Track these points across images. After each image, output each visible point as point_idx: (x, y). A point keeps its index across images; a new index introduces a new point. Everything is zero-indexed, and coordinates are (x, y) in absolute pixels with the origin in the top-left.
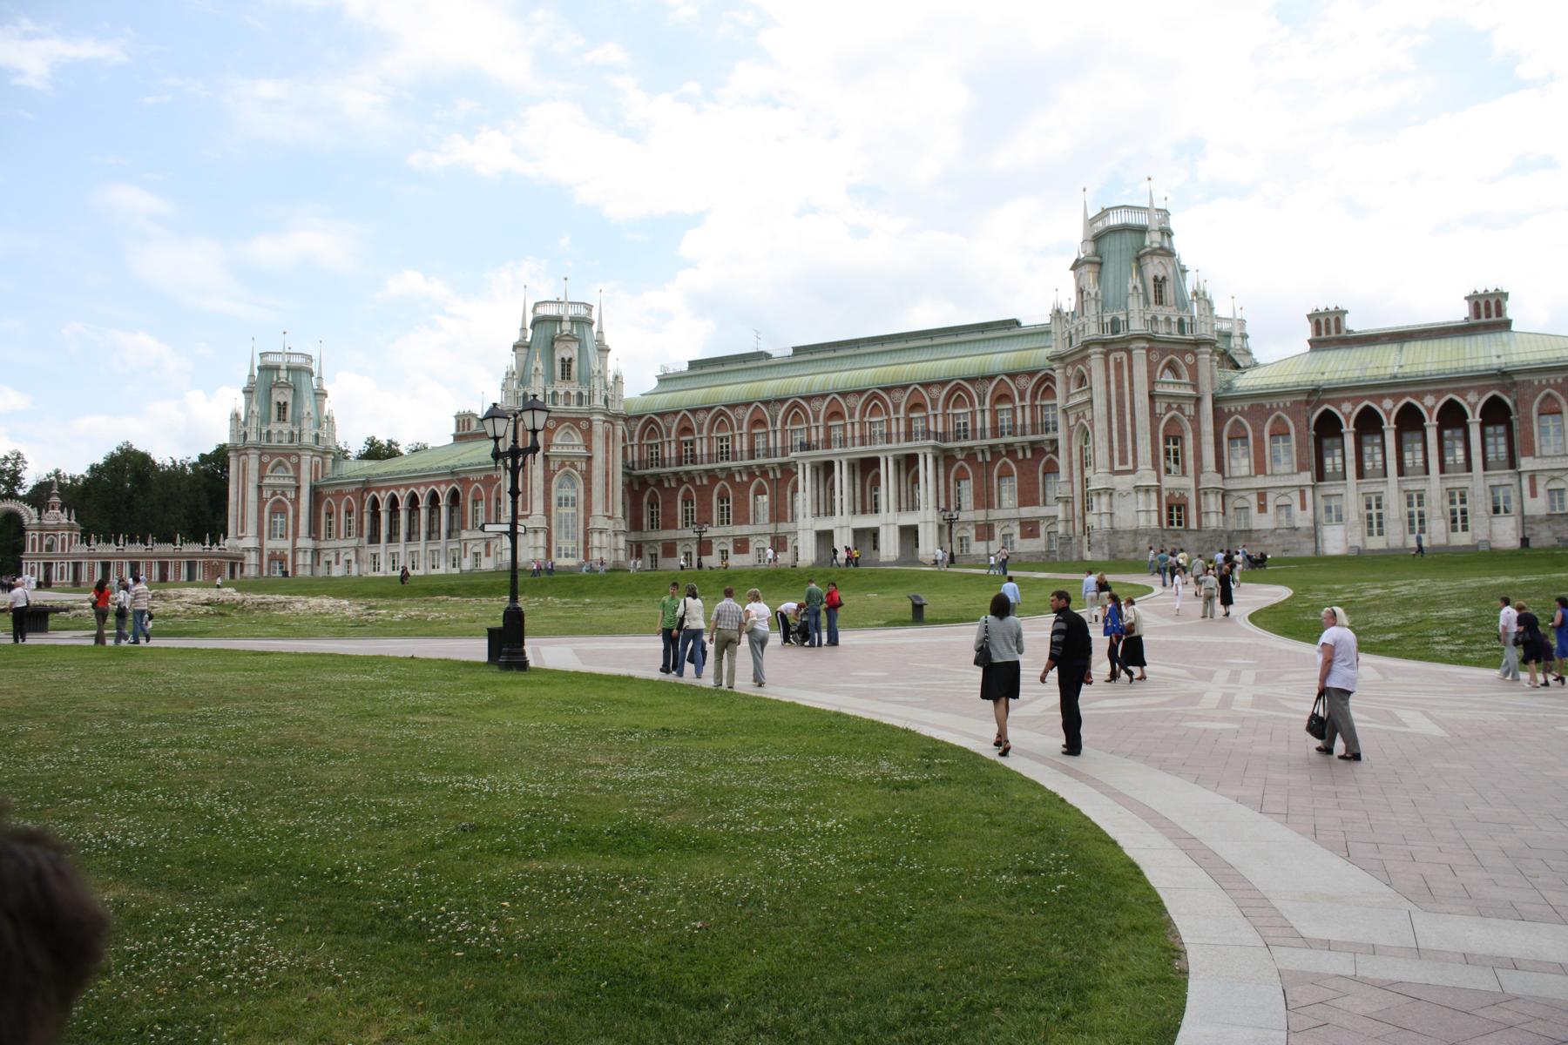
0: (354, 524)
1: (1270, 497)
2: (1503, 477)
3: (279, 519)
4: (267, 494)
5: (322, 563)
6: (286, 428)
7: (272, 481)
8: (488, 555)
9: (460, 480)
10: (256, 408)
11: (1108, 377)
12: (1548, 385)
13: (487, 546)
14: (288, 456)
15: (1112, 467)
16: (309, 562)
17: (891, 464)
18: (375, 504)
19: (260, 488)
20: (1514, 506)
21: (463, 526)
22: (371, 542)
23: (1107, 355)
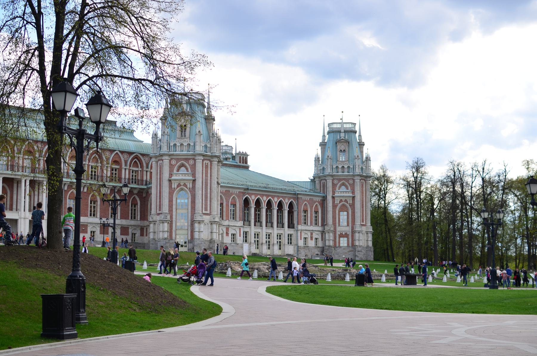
1: (230, 229)
2: (291, 231)
11: (203, 170)
12: (306, 200)
15: (202, 211)
17: (28, 183)
20: (294, 241)
23: (203, 160)
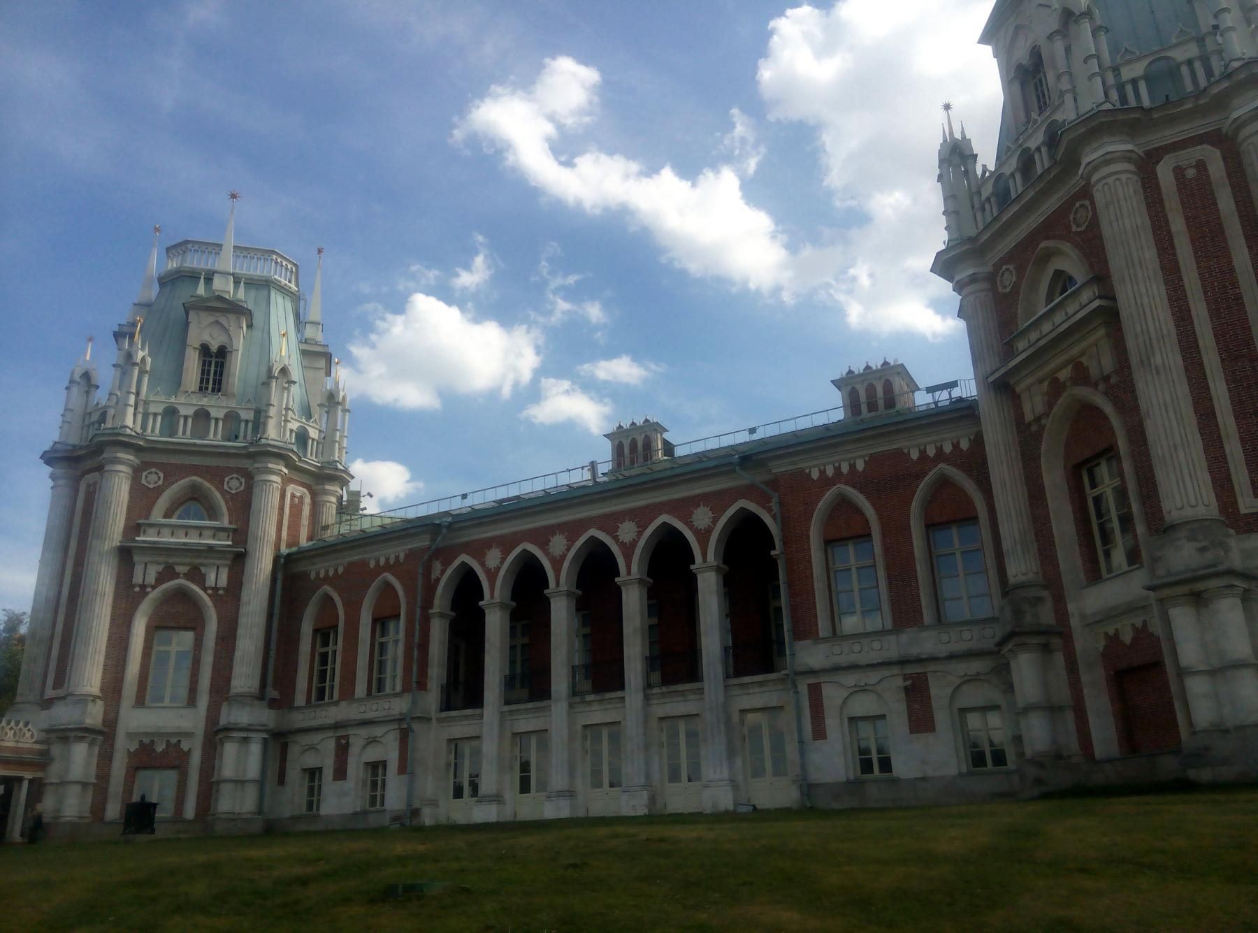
3: (174, 648)
4: (145, 572)
6: (217, 407)
7: (166, 539)
8: (921, 721)
9: (774, 483)
13: (916, 692)
14: (217, 475)
16: (253, 771)
21: (805, 631)
22: (447, 705)
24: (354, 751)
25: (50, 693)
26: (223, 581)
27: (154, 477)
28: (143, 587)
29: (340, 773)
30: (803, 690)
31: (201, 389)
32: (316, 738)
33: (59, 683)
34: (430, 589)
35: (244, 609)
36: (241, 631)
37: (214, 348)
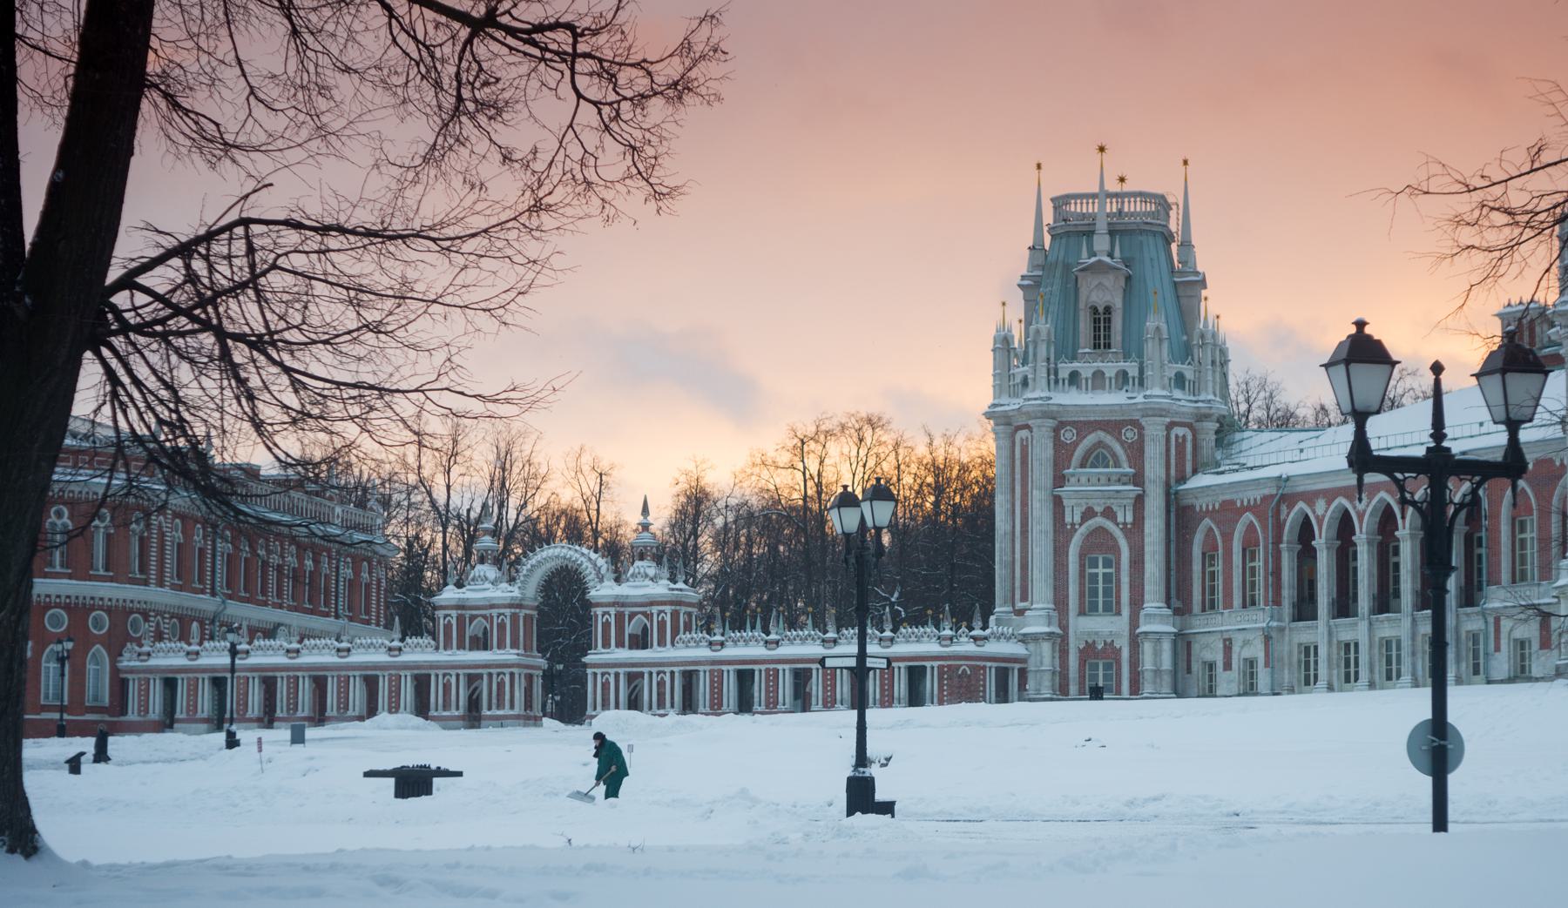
0: (1260, 578)
3: (1101, 570)
4: (1072, 516)
5: (1195, 667)
10: (1044, 326)
16: (1167, 663)
18: (1306, 531)
19: (1058, 502)
24: (1236, 649)
25: (1020, 605)
26: (1129, 519)
27: (1068, 435)
28: (1073, 524)
29: (1228, 666)
30: (1491, 620)
31: (1096, 346)
32: (1211, 638)
33: (1024, 598)
34: (1279, 527)
35: (1147, 540)
36: (1147, 557)
37: (1101, 310)
